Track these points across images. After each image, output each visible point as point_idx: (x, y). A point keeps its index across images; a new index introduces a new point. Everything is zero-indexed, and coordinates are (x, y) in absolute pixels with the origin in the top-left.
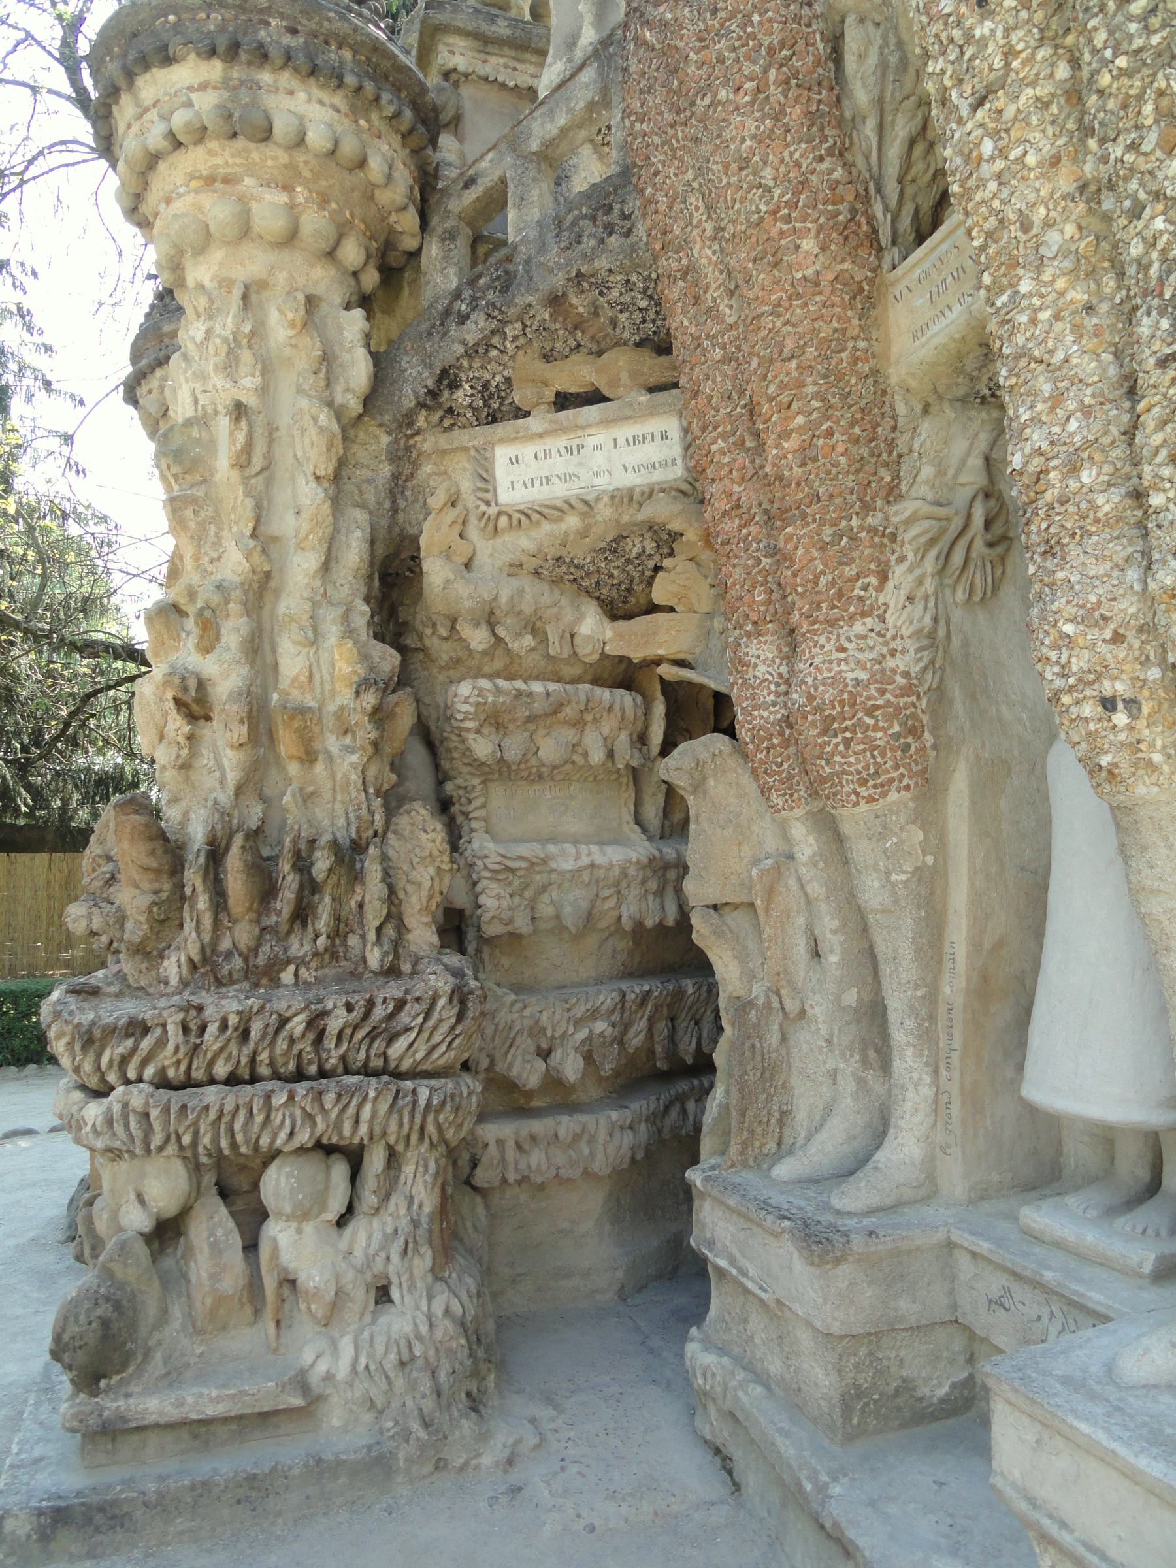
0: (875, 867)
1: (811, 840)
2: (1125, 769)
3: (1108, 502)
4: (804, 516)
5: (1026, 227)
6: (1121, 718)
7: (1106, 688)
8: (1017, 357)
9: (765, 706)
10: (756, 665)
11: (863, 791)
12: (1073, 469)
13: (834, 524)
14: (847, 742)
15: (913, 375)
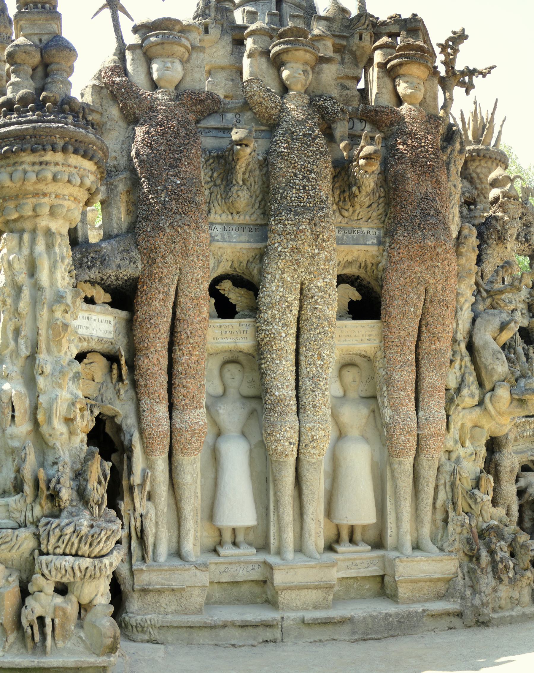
0: (191, 473)
1: (163, 464)
2: (289, 455)
3: (295, 408)
4: (194, 378)
5: (287, 352)
6: (292, 446)
7: (291, 440)
8: (280, 374)
9: (163, 425)
10: (158, 412)
11: (196, 453)
12: (290, 401)
13: (200, 382)
14: (197, 440)
15: (212, 348)
